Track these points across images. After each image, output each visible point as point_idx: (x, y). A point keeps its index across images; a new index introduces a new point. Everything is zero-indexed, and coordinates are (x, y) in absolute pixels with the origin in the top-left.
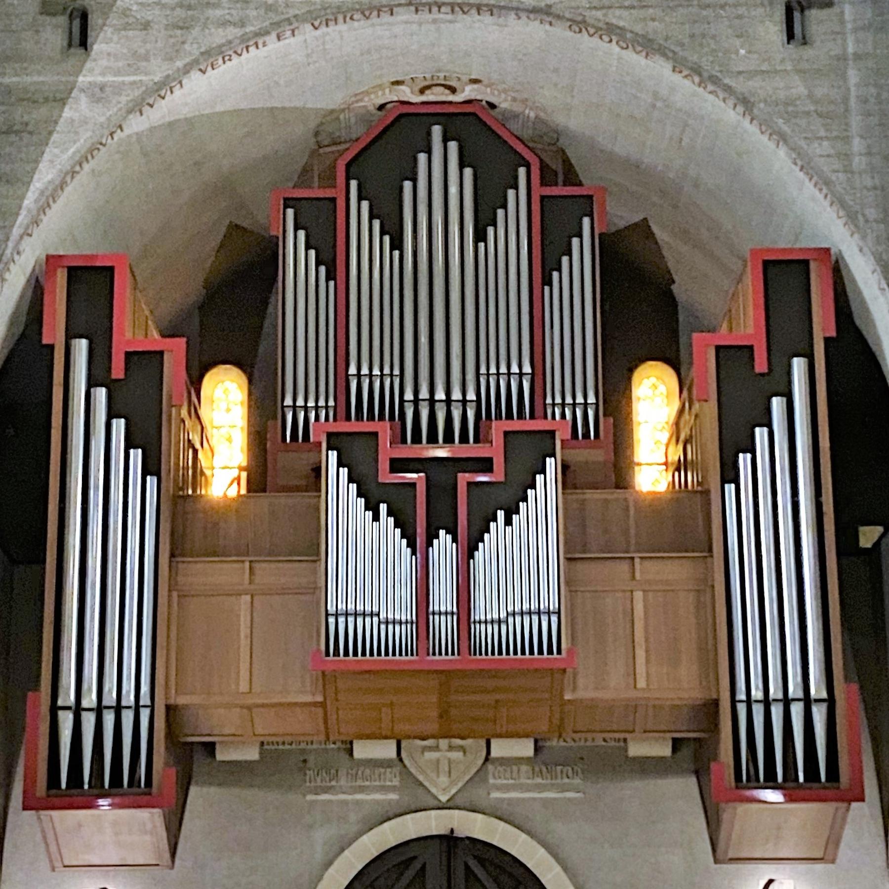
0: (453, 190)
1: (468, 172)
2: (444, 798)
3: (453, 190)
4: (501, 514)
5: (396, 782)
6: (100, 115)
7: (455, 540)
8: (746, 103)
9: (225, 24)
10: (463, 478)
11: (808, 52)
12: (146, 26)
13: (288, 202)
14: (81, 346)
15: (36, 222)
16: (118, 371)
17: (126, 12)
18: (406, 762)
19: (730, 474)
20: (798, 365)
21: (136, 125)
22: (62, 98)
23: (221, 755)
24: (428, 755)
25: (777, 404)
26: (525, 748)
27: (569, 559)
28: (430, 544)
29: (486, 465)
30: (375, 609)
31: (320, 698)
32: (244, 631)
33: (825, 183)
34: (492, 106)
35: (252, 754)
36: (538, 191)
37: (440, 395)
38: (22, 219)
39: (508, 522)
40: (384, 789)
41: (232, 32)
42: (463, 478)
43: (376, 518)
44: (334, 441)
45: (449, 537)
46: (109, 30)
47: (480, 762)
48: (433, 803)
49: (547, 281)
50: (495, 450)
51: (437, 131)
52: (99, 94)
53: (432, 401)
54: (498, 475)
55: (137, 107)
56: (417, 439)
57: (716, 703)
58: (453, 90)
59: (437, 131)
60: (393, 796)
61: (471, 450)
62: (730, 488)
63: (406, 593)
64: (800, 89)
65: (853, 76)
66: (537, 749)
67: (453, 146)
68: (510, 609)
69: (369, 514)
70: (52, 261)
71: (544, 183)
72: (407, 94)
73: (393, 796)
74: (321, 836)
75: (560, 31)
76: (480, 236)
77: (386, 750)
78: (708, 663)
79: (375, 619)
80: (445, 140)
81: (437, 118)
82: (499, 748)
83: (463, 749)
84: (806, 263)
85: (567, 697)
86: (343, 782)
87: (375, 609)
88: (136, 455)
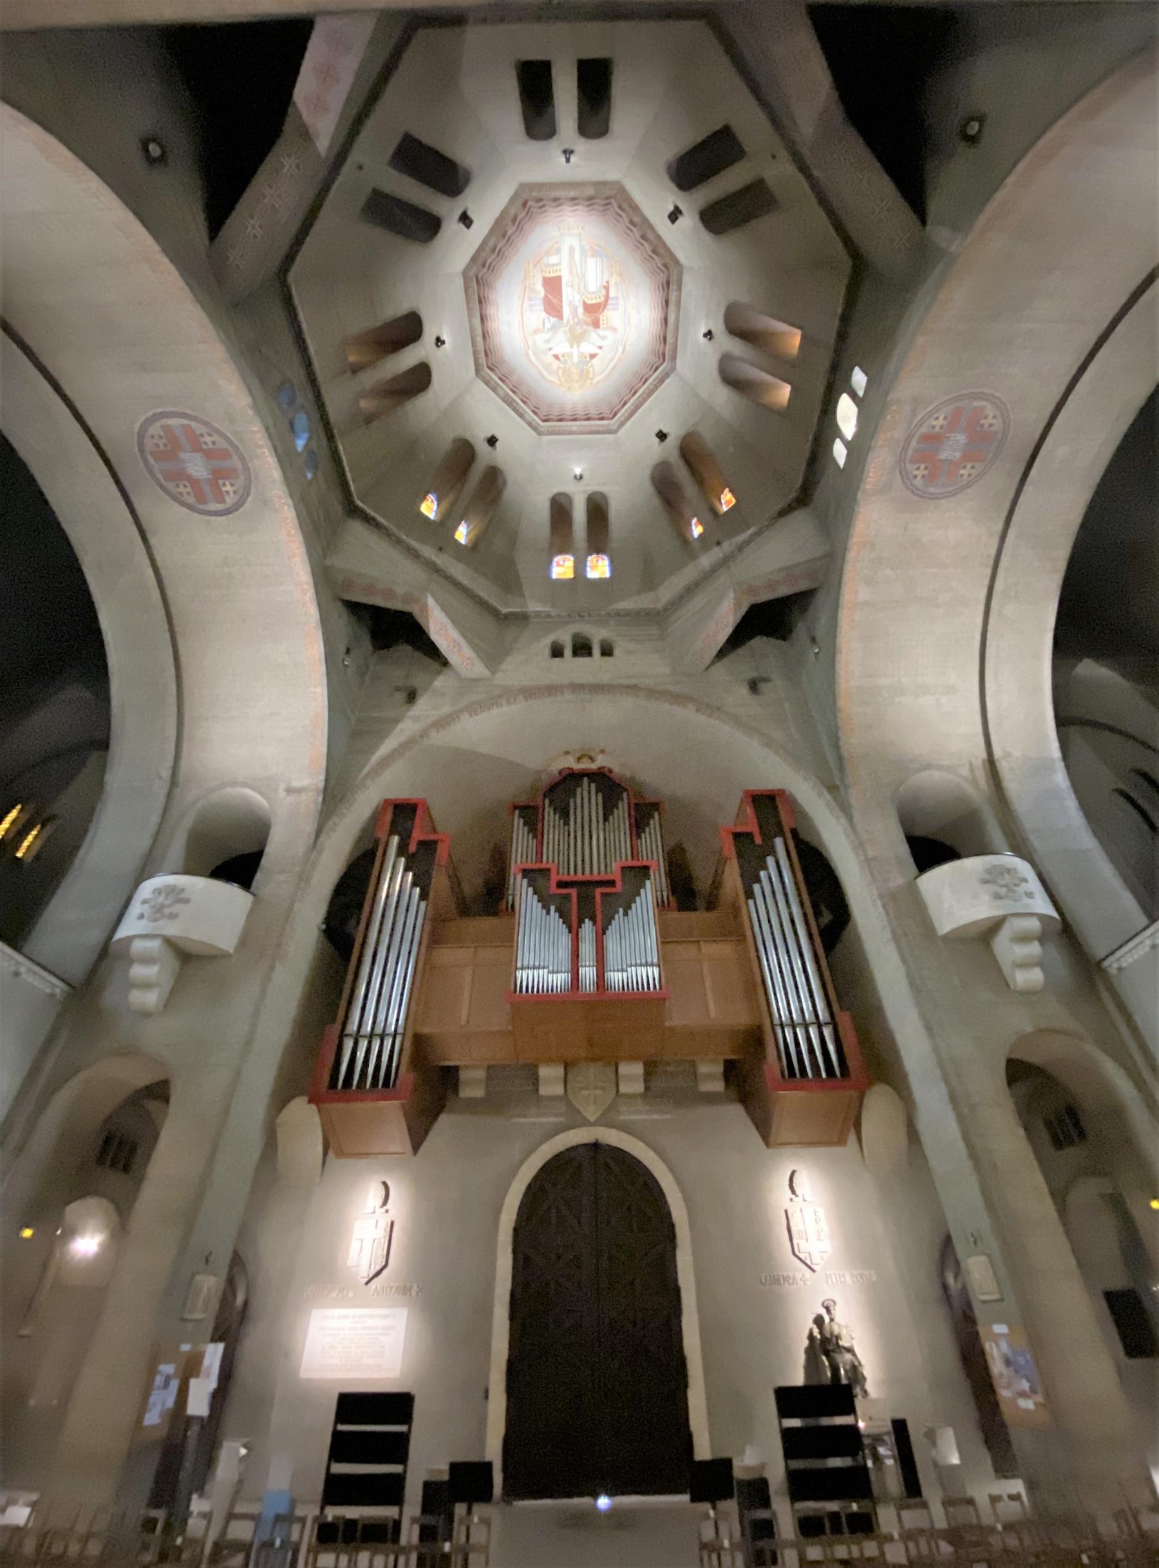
1: (600, 795)
2: (592, 1119)
4: (621, 910)
5: (564, 1109)
7: (594, 924)
10: (599, 891)
14: (395, 839)
16: (413, 848)
18: (570, 1097)
19: (750, 894)
20: (779, 842)
22: (397, 721)
24: (585, 1093)
27: (663, 943)
28: (579, 926)
29: (611, 883)
30: (546, 964)
31: (510, 1028)
34: (610, 771)
35: (479, 1093)
38: (366, 770)
39: (626, 914)
40: (556, 1115)
43: (548, 913)
45: (591, 923)
46: (425, 696)
47: (613, 1096)
51: (586, 780)
52: (416, 719)
58: (592, 759)
59: (586, 780)
60: (561, 1119)
62: (751, 902)
65: (787, 706)
66: (647, 1088)
68: (629, 963)
69: (544, 911)
72: (571, 763)
73: (561, 1119)
76: (606, 819)
79: (546, 971)
83: (603, 1089)
85: (667, 1024)
87: (546, 964)
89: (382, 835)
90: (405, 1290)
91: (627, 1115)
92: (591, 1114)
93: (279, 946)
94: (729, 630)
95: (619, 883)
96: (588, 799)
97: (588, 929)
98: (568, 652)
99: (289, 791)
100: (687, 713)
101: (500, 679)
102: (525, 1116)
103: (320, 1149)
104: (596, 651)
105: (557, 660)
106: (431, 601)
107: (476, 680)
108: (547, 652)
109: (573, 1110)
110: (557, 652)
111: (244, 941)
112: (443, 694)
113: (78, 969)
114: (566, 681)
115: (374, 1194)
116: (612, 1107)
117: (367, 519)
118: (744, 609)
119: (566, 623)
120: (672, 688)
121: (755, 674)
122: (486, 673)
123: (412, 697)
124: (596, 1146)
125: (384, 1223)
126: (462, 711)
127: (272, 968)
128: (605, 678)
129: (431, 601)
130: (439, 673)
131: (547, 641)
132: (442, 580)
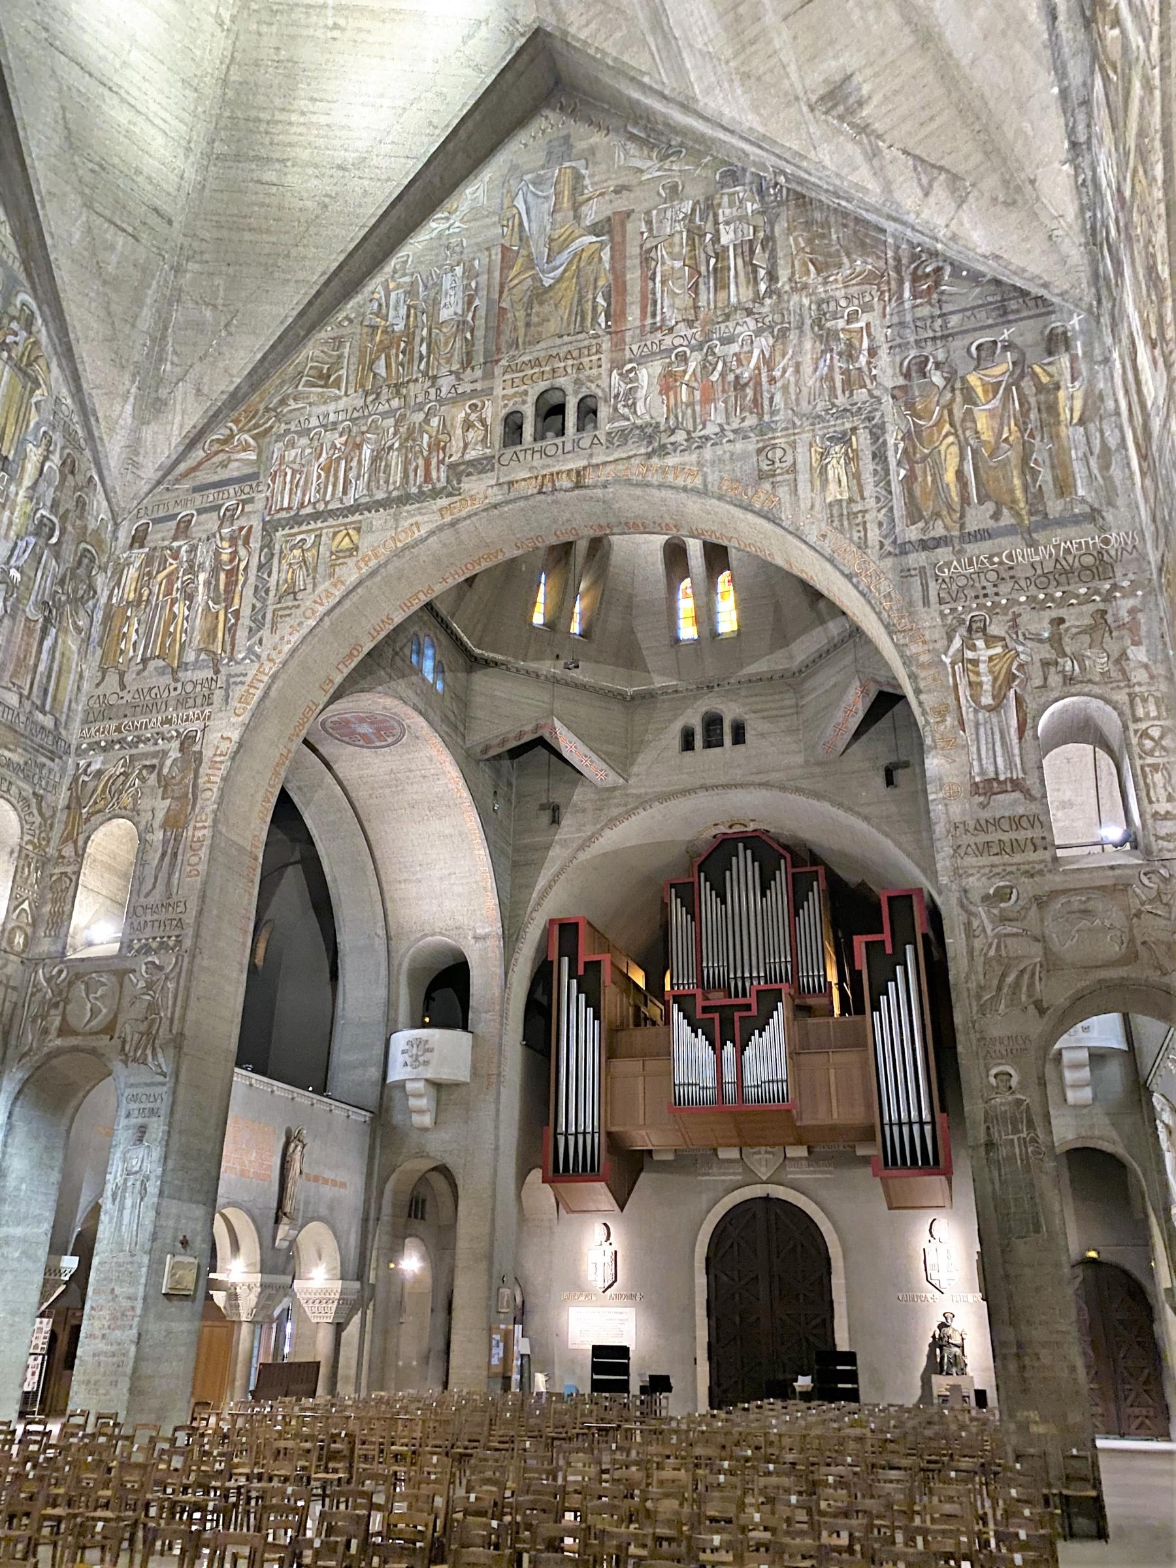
0: (750, 874)
3: (750, 874)
6: (566, 853)
8: (866, 818)
9: (618, 805)
10: (737, 1015)
11: (897, 791)
12: (584, 811)
13: (672, 886)
15: (539, 904)
16: (581, 972)
17: (575, 805)
19: (876, 1007)
21: (583, 856)
23: (656, 1157)
24: (757, 1157)
25: (899, 969)
26: (802, 1152)
29: (748, 1007)
32: (641, 1095)
33: (909, 855)
35: (670, 1157)
36: (791, 870)
37: (747, 975)
40: (734, 1174)
41: (622, 809)
42: (737, 1015)
44: (677, 999)
48: (757, 1179)
49: (797, 914)
50: (752, 1000)
51: (741, 845)
52: (564, 843)
53: (743, 978)
54: (754, 1011)
55: (581, 848)
56: (736, 996)
57: (873, 1127)
59: (741, 845)
61: (741, 1001)
63: (711, 1072)
64: (893, 809)
66: (809, 1152)
67: (749, 852)
70: (552, 921)
71: (794, 866)
72: (723, 829)
74: (705, 1199)
75: (776, 793)
76: (763, 895)
77: (734, 1154)
78: (869, 1106)
80: (745, 849)
81: (742, 839)
82: (792, 1152)
84: (910, 897)
86: (715, 1170)
88: (590, 1011)
89: (554, 955)
90: (631, 1297)
91: (794, 1174)
92: (764, 1173)
93: (499, 1075)
94: (860, 716)
95: (754, 1007)
96: (744, 867)
97: (729, 1050)
98: (699, 741)
99: (477, 938)
100: (826, 807)
101: (636, 787)
102: (708, 1174)
103: (553, 1200)
104: (728, 739)
105: (689, 753)
106: (557, 723)
107: (614, 789)
108: (676, 742)
109: (748, 1170)
110: (688, 743)
111: (475, 1072)
112: (584, 811)
113: (372, 1099)
114: (698, 783)
115: (599, 1232)
116: (782, 1165)
117: (487, 663)
118: (873, 695)
119: (696, 698)
120: (804, 784)
121: (893, 759)
122: (621, 781)
123: (555, 814)
124: (767, 1199)
125: (610, 1250)
126: (602, 829)
127: (499, 1093)
128: (738, 775)
129: (557, 723)
130: (575, 784)
131: (676, 728)
132: (563, 690)
